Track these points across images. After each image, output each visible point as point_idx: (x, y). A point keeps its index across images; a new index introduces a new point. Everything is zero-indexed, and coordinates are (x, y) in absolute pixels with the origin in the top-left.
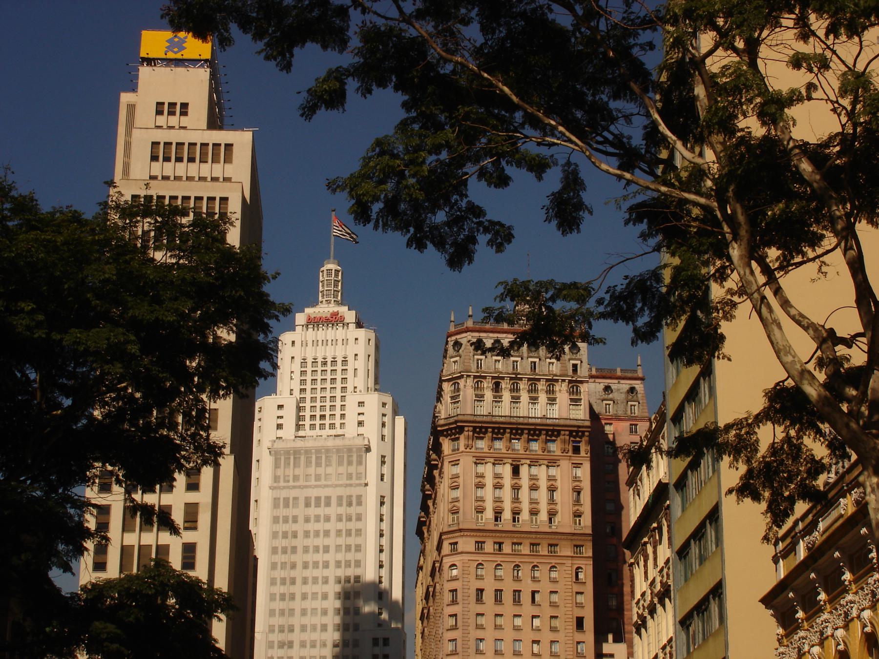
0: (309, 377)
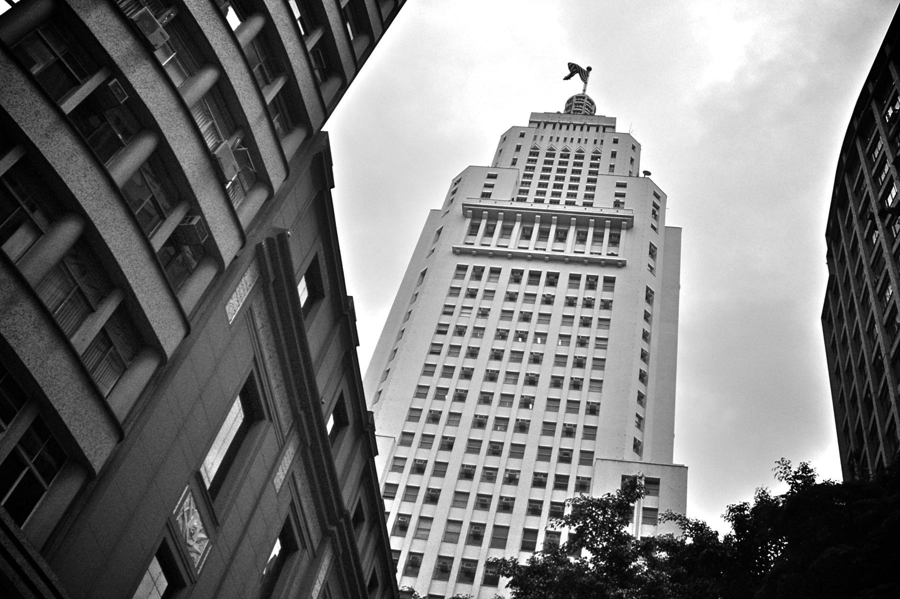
0: (540, 165)
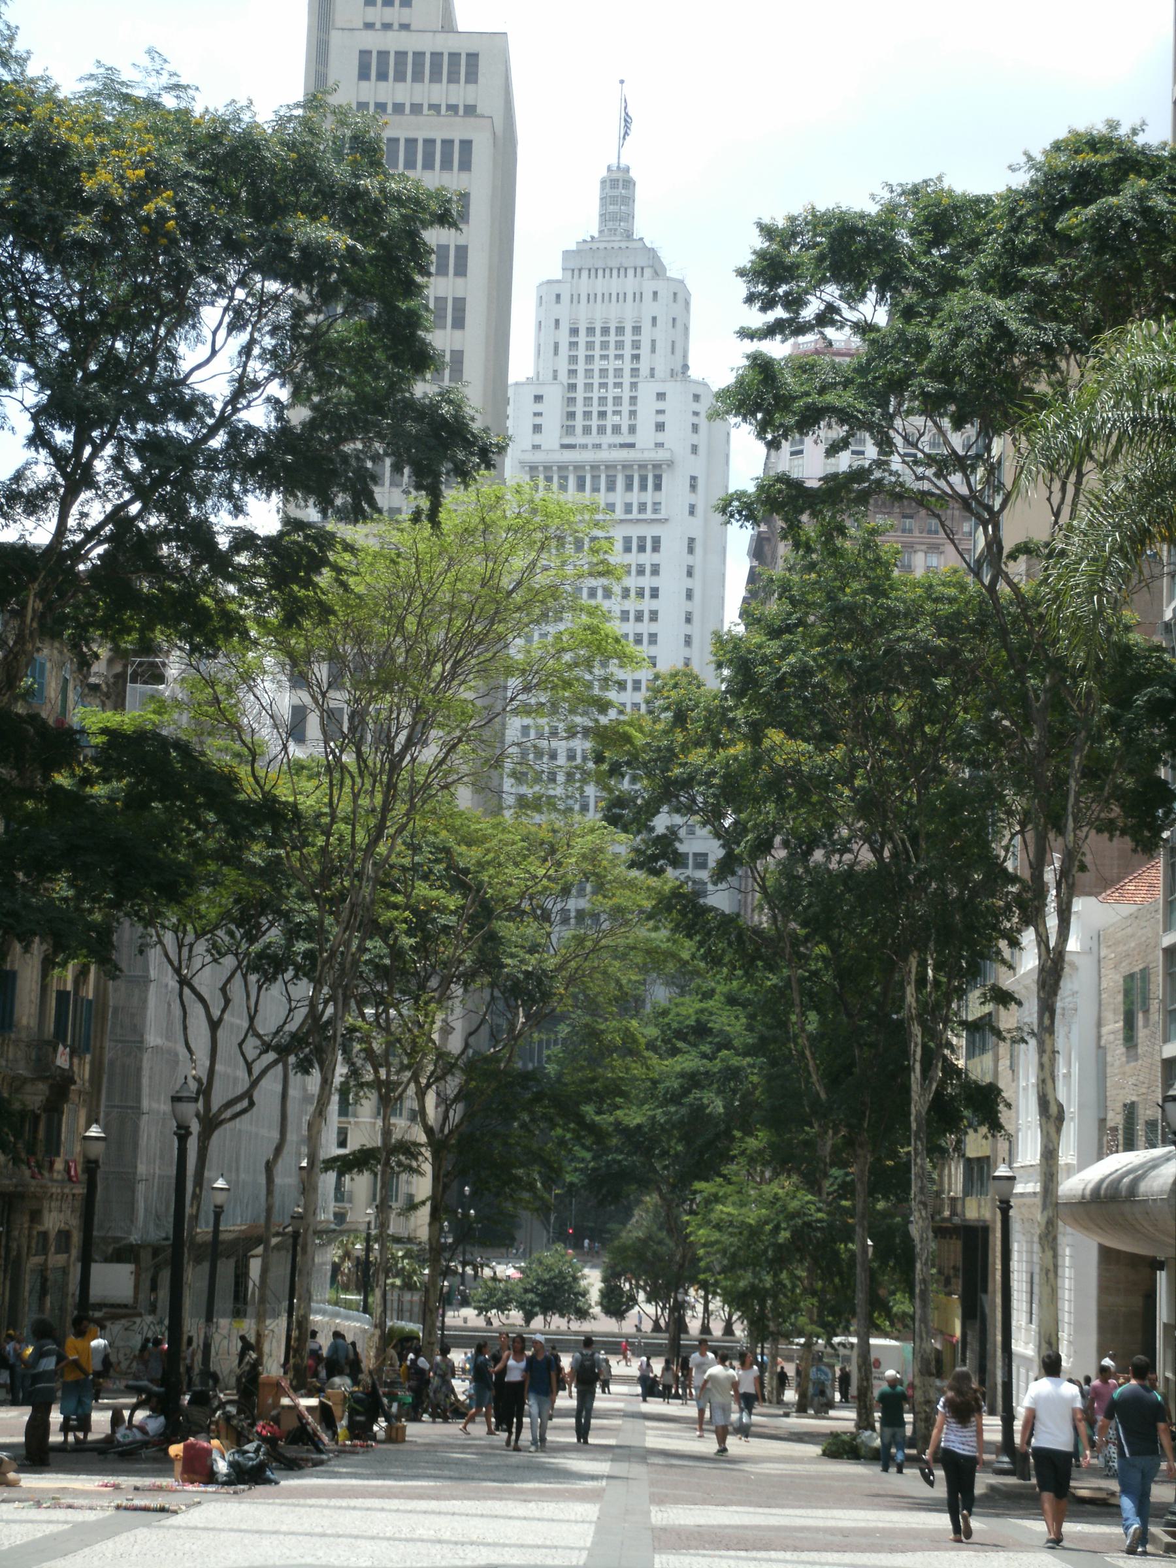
0: (582, 352)
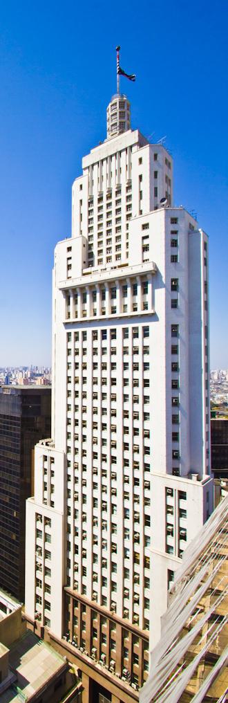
0: (95, 215)
